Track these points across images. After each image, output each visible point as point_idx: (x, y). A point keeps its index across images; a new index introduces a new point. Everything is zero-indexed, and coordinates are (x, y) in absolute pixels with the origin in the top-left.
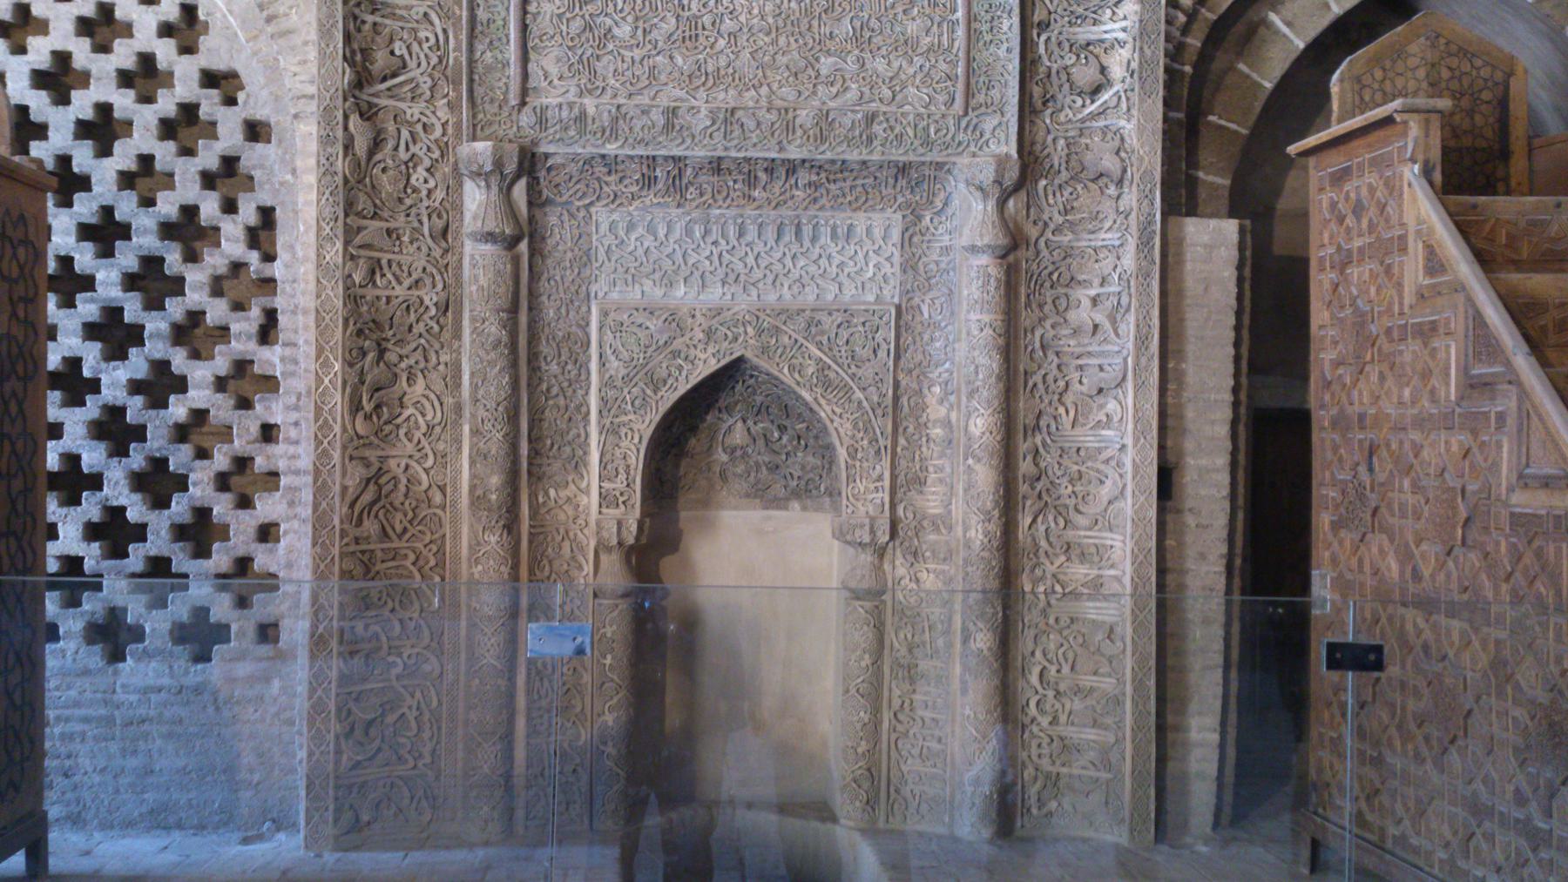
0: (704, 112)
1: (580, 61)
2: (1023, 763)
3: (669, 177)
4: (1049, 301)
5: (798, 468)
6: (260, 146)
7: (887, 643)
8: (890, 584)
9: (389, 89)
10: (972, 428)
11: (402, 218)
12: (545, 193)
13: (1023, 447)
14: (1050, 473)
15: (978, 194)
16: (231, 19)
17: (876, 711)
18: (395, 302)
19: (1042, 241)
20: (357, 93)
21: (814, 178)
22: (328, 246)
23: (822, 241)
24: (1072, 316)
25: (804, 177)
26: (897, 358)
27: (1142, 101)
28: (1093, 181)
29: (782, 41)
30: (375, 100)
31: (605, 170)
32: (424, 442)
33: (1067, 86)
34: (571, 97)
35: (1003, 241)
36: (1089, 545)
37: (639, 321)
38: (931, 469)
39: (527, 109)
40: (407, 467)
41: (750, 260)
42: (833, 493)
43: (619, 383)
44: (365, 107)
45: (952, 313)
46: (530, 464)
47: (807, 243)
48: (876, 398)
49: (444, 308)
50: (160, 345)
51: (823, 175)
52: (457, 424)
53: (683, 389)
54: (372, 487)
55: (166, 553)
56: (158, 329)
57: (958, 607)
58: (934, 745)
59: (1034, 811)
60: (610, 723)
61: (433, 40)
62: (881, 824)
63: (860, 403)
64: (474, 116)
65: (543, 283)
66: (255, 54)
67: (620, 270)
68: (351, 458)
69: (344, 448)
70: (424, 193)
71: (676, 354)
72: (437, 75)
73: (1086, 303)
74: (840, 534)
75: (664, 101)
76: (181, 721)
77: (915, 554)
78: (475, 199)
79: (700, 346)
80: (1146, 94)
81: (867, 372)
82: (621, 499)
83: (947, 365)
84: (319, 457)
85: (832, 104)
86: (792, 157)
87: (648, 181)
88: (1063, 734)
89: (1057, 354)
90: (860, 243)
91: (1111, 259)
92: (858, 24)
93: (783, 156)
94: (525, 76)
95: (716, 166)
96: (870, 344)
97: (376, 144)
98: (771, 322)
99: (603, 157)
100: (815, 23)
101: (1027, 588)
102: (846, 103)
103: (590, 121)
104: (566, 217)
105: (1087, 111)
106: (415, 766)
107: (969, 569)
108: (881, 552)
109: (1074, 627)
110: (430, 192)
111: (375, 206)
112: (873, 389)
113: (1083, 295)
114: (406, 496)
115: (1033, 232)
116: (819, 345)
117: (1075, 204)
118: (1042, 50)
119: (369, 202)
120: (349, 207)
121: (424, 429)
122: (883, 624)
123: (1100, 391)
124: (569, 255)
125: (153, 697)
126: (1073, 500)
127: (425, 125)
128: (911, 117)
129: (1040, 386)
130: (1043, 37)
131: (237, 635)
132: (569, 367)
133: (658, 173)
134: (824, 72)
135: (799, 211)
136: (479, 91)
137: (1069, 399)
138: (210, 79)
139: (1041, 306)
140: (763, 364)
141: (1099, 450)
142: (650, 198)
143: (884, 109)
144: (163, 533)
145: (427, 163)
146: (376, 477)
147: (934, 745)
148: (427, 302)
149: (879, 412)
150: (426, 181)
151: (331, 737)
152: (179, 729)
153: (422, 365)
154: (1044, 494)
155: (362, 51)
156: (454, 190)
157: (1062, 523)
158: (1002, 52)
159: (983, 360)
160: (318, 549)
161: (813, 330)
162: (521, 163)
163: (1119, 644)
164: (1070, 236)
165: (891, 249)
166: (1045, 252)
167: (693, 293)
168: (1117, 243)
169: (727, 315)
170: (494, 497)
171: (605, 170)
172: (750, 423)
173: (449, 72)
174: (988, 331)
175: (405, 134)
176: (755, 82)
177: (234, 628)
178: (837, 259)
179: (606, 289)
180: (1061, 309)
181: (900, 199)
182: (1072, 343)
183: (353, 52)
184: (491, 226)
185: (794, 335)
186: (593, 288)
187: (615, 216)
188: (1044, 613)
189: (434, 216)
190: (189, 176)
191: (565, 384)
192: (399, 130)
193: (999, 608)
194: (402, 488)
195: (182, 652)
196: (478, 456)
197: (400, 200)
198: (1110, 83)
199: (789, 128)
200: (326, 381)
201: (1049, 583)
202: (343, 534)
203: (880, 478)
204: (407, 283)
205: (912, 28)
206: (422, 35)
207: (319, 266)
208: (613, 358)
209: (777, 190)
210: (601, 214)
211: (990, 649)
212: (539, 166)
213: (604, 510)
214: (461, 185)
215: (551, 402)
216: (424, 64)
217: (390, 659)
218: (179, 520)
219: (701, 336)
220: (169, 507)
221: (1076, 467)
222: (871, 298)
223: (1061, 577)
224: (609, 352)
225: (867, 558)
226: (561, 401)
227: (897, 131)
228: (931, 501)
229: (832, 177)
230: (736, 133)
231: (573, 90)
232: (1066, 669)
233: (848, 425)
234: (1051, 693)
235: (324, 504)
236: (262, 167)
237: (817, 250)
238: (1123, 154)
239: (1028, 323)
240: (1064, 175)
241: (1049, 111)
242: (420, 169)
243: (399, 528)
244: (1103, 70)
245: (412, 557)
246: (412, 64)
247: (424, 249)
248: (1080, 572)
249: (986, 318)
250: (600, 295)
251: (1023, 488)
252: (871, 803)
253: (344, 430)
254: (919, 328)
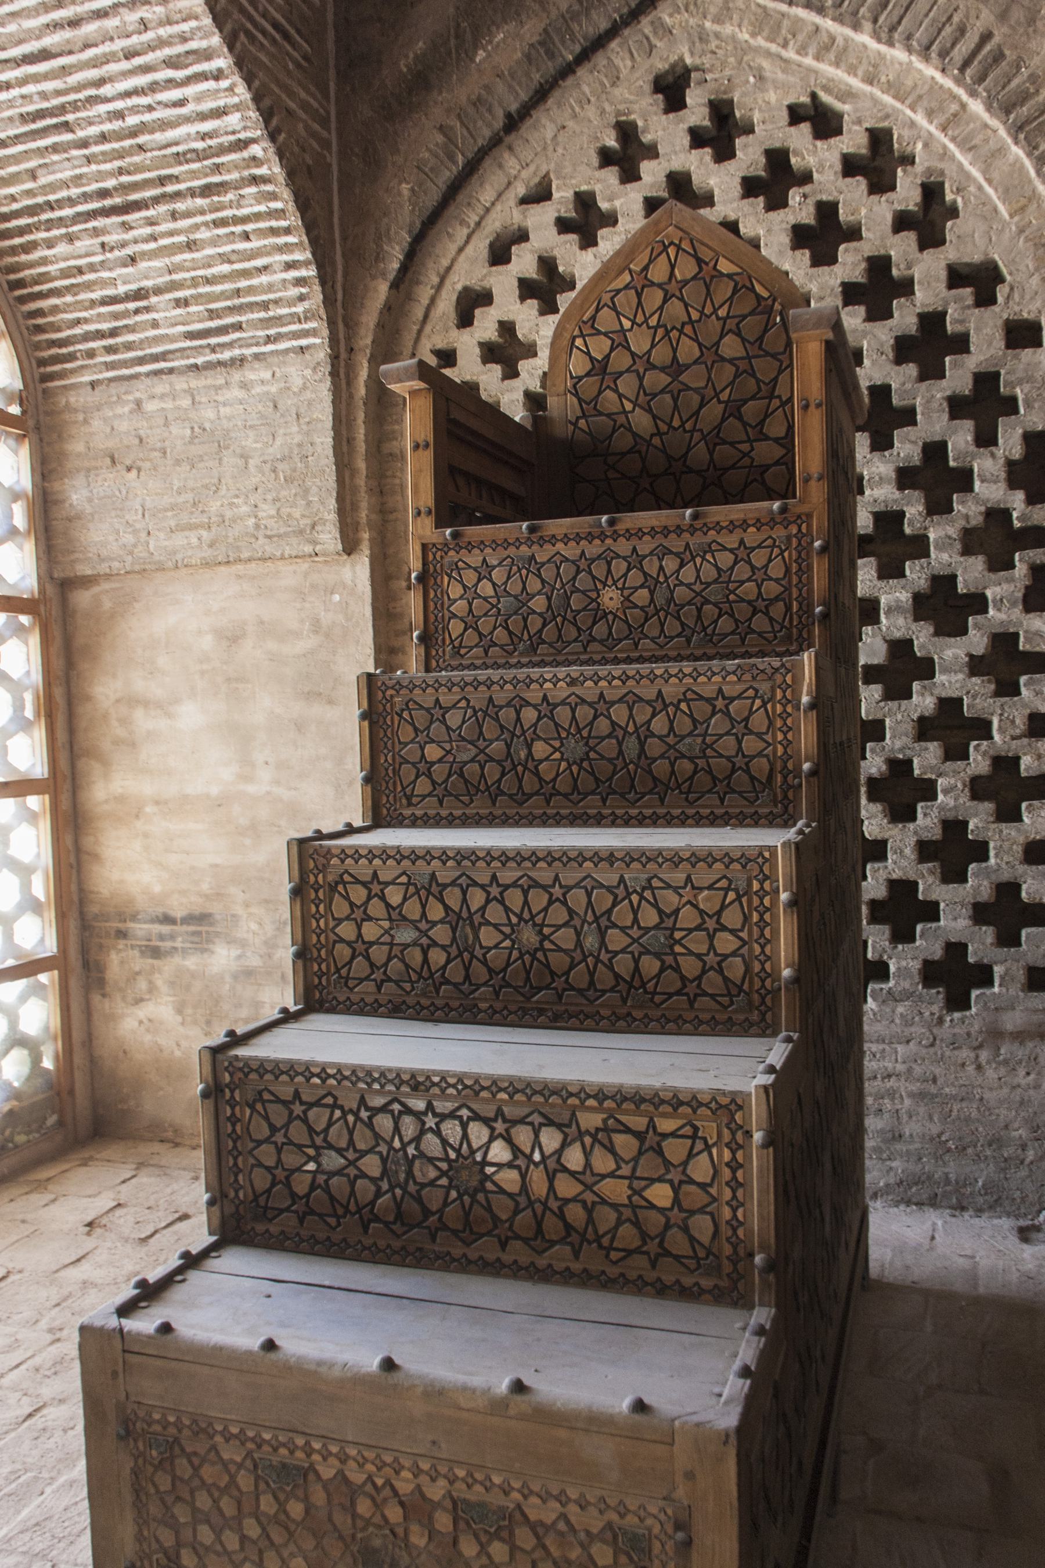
16: (990, 190)
50: (901, 621)
55: (912, 876)
56: (898, 600)
66: (1021, 231)
76: (934, 1080)
125: (900, 1048)
131: (1002, 978)
138: (957, 277)
144: (908, 851)
152: (933, 1089)
177: (998, 970)
190: (935, 405)
195: (937, 996)
218: (926, 836)
220: (914, 819)
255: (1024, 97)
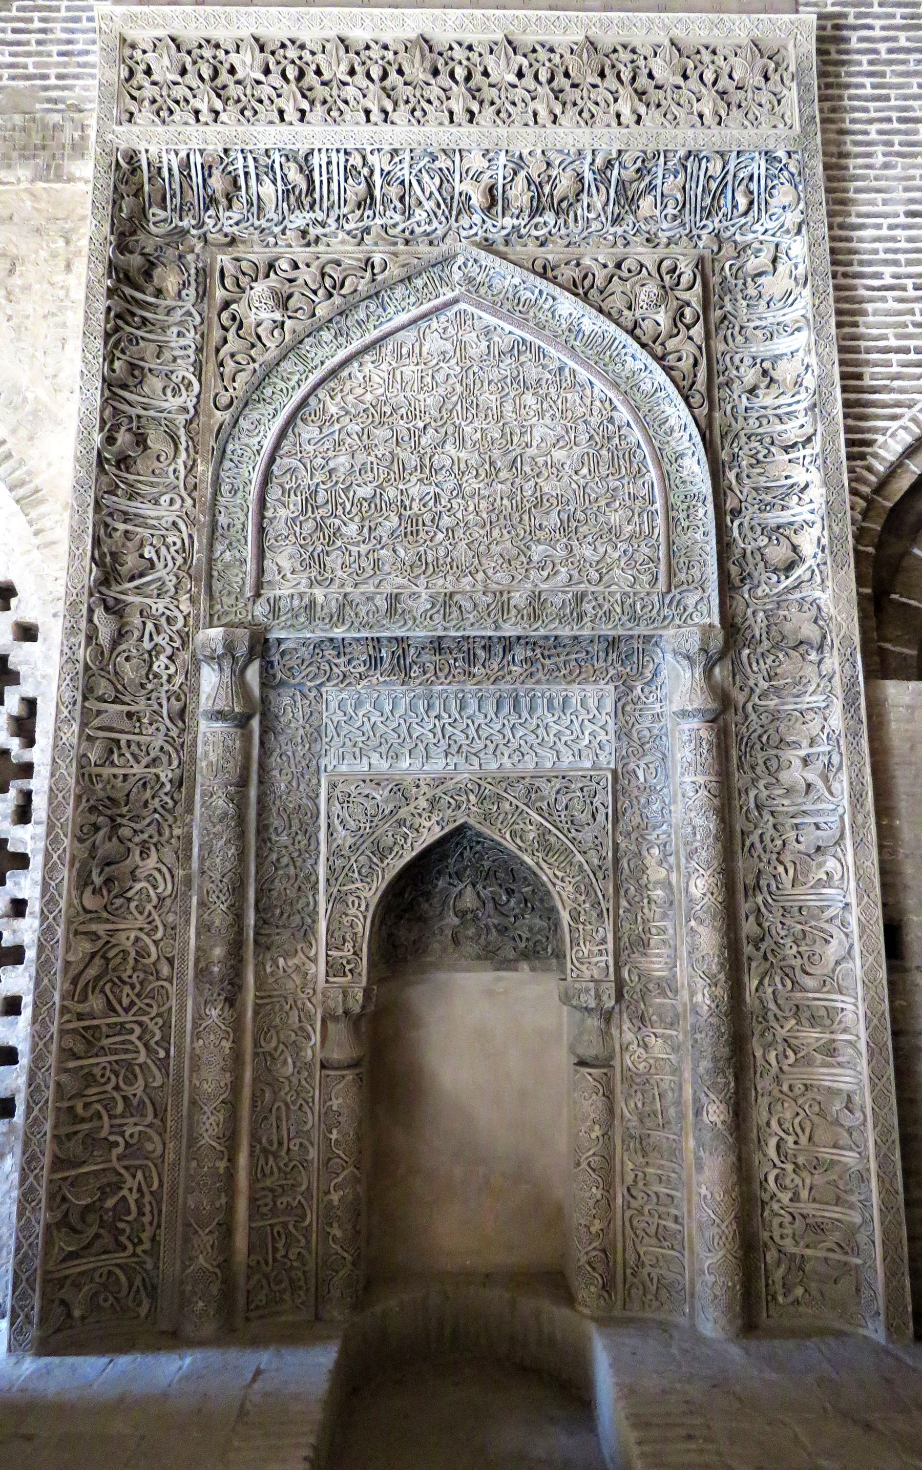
0: (424, 596)
1: (311, 556)
2: (765, 1245)
3: (395, 658)
4: (761, 761)
5: (522, 930)
6: (28, 645)
7: (618, 1112)
8: (617, 1047)
9: (137, 588)
10: (692, 889)
11: (143, 702)
12: (279, 675)
13: (745, 907)
14: (774, 932)
15: (685, 663)
17: (608, 1187)
18: (132, 780)
19: (750, 705)
20: (104, 589)
21: (529, 653)
22: (65, 728)
23: (539, 712)
24: (784, 776)
25: (520, 653)
26: (616, 821)
27: (835, 573)
28: (794, 648)
29: (496, 533)
30: (123, 597)
31: (335, 653)
32: (155, 915)
33: (762, 564)
34: (302, 588)
35: (712, 705)
36: (818, 1007)
37: (366, 792)
38: (654, 931)
39: (262, 600)
40: (137, 939)
41: (472, 732)
42: (559, 955)
43: (346, 852)
44: (111, 602)
45: (667, 776)
46: (257, 934)
47: (525, 714)
48: (596, 861)
49: (178, 783)
51: (538, 651)
52: (187, 897)
53: (408, 856)
54: (98, 961)
57: (687, 1075)
58: (671, 1224)
59: (780, 1299)
60: (336, 1203)
61: (179, 543)
62: (617, 1312)
63: (581, 866)
64: (211, 607)
65: (274, 760)
67: (348, 743)
68: (76, 933)
69: (69, 922)
70: (165, 678)
71: (401, 823)
72: (181, 574)
73: (797, 763)
74: (566, 998)
75: (387, 589)
77: (642, 1019)
78: (210, 680)
79: (425, 815)
80: (839, 566)
81: (586, 835)
82: (348, 967)
83: (664, 827)
84: (43, 933)
85: (543, 586)
86: (507, 634)
87: (375, 662)
88: (805, 1212)
89: (772, 813)
90: (575, 713)
91: (818, 720)
92: (564, 516)
93: (498, 634)
94: (261, 571)
95: (437, 645)
96: (589, 809)
97: (120, 635)
98: (491, 791)
99: (331, 640)
100: (526, 517)
101: (759, 1054)
102: (556, 586)
103: (319, 608)
104: (298, 697)
105: (782, 586)
106: (134, 1255)
107: (698, 1036)
108: (607, 1017)
109: (810, 1095)
110: (170, 676)
111: (117, 691)
112: (593, 852)
113: (793, 756)
114: (134, 970)
115: (740, 698)
116: (539, 811)
117: (778, 670)
118: (736, 533)
119: (110, 687)
120: (88, 692)
121: (155, 900)
122: (612, 1092)
123: (818, 848)
124: (301, 732)
126: (799, 960)
127: (168, 618)
128: (618, 596)
129: (758, 845)
130: (736, 523)
132: (299, 837)
133: (384, 654)
134: (535, 558)
135: (517, 685)
136: (217, 586)
137: (787, 857)
139: (753, 768)
140: (486, 831)
141: (822, 909)
142: (376, 677)
143: (593, 589)
145: (169, 651)
146: (103, 952)
147: (671, 1224)
148: (163, 779)
149: (600, 875)
150: (167, 668)
151: (40, 1229)
153: (155, 840)
154: (769, 955)
155: (111, 554)
156: (192, 673)
157: (789, 984)
158: (699, 536)
159: (699, 821)
160: (37, 1027)
161: (533, 796)
162: (251, 649)
163: (858, 1114)
164: (777, 701)
165: (604, 717)
166: (753, 717)
167: (418, 764)
168: (823, 705)
169: (450, 784)
170: (216, 969)
171: (335, 653)
172: (479, 887)
173: (192, 571)
174: (703, 792)
175: (150, 626)
176: (472, 569)
178: (554, 728)
179: (334, 763)
180: (773, 770)
181: (612, 672)
182: (786, 802)
183: (103, 555)
184: (221, 705)
185: (515, 802)
186: (323, 762)
187: (344, 695)
188: (777, 1080)
189: (173, 699)
191: (295, 854)
192: (144, 623)
193: (731, 1078)
194: (131, 962)
196: (204, 928)
197: (142, 686)
198: (802, 560)
199: (504, 608)
200: (55, 857)
201: (780, 1048)
202: (64, 1010)
203: (604, 941)
204: (144, 762)
205: (615, 518)
206: (170, 540)
207: (55, 746)
208: (340, 828)
209: (495, 666)
210: (331, 693)
211: (724, 1122)
212: (273, 651)
213: (331, 979)
214: (198, 670)
215: (280, 872)
216: (170, 564)
217: (112, 1138)
219: (425, 804)
221: (799, 927)
222: (589, 765)
223: (793, 1041)
224: (336, 822)
225: (593, 1022)
226: (292, 871)
227: (605, 608)
228: (656, 964)
229: (546, 653)
230: (454, 615)
231: (304, 581)
232: (804, 1140)
233: (570, 888)
234: (789, 1167)
235: (46, 981)
236: (27, 662)
237: (535, 721)
238: (821, 623)
239: (740, 784)
240: (766, 644)
241: (747, 587)
242: (162, 657)
243: (126, 1002)
244: (795, 548)
245: (138, 1031)
246: (159, 565)
247: (163, 729)
248: (812, 1036)
249: (701, 779)
250: (330, 768)
251: (748, 949)
252: (607, 1287)
253: (70, 905)
254: (636, 792)
255: (22, 484)
